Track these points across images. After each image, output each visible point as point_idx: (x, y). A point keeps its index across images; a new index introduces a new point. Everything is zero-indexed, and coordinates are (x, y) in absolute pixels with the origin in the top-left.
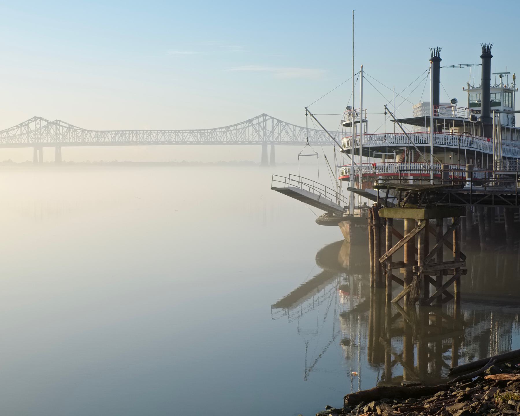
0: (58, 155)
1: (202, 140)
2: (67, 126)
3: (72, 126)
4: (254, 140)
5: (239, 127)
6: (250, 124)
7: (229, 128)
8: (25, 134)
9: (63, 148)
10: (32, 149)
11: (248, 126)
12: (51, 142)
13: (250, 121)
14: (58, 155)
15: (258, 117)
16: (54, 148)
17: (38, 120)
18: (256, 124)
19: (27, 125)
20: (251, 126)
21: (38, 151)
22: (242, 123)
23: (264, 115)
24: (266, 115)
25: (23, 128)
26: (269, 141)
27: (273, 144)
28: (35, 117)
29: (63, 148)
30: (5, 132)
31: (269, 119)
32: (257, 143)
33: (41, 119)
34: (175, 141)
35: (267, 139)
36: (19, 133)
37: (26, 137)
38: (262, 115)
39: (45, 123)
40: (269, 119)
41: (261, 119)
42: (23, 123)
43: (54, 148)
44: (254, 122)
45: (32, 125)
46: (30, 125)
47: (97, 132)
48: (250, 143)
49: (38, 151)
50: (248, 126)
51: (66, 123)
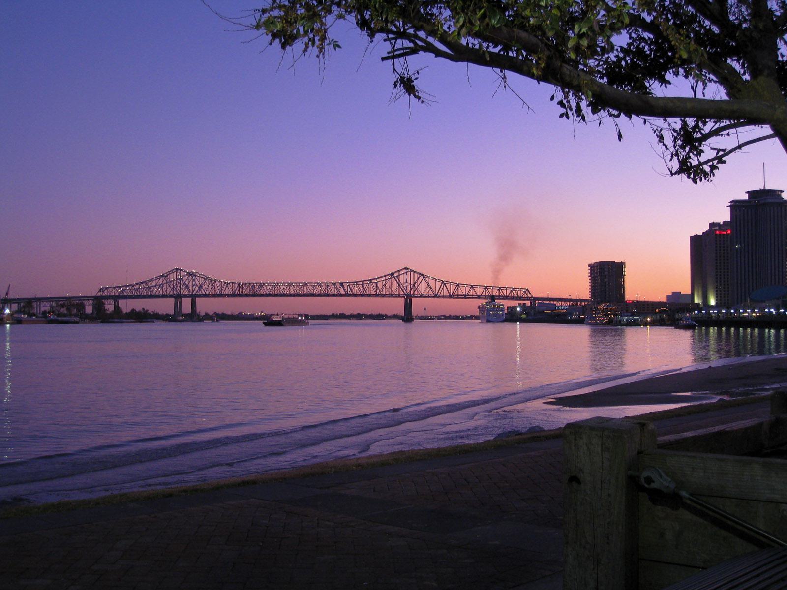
0: (194, 304)
4: (331, 293)
8: (165, 283)
10: (173, 300)
13: (392, 274)
14: (194, 304)
16: (190, 299)
17: (179, 271)
23: (406, 269)
25: (163, 278)
27: (414, 296)
32: (399, 296)
33: (181, 270)
34: (275, 294)
37: (170, 289)
41: (405, 271)
42: (162, 276)
43: (190, 299)
45: (172, 277)
48: (392, 296)
50: (391, 278)
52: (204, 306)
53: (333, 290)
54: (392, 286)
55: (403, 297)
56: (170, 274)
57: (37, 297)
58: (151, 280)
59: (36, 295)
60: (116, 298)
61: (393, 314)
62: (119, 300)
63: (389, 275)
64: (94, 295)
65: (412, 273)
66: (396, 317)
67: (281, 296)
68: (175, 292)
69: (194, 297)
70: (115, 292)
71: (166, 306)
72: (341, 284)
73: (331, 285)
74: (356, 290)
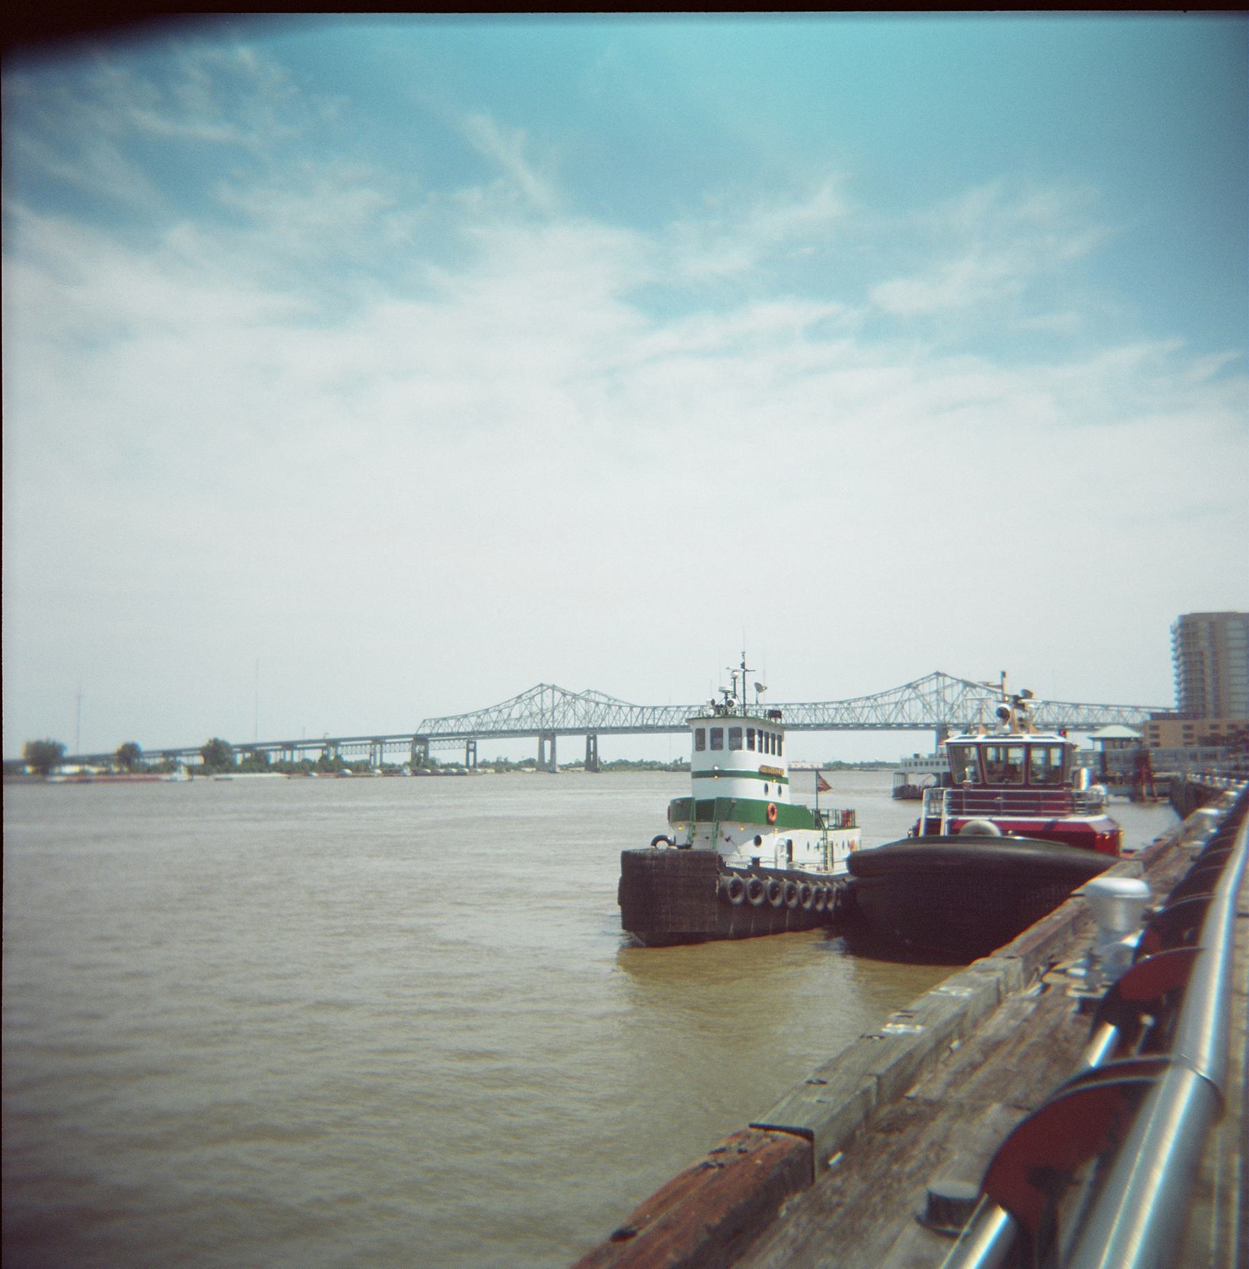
2: (604, 700)
6: (913, 695)
7: (875, 700)
9: (600, 738)
11: (909, 699)
15: (927, 679)
16: (583, 738)
18: (931, 693)
19: (532, 698)
20: (914, 699)
21: (547, 744)
22: (896, 691)
23: (938, 674)
24: (945, 675)
28: (541, 685)
29: (600, 738)
30: (495, 711)
31: (951, 686)
32: (928, 727)
33: (553, 688)
36: (515, 714)
39: (558, 695)
40: (951, 686)
42: (520, 697)
43: (583, 738)
45: (538, 698)
46: (536, 698)
48: (914, 726)
49: (547, 744)
51: (605, 696)
52: (610, 748)
54: (915, 712)
55: (933, 728)
56: (923, 683)
57: (328, 737)
58: (882, 695)
59: (327, 734)
60: (470, 738)
61: (455, 762)
62: (478, 741)
63: (909, 686)
64: (413, 732)
65: (597, 695)
66: (578, 764)
67: (814, 729)
68: (813, 719)
69: (592, 734)
70: (467, 726)
71: (527, 748)
73: (1100, 710)
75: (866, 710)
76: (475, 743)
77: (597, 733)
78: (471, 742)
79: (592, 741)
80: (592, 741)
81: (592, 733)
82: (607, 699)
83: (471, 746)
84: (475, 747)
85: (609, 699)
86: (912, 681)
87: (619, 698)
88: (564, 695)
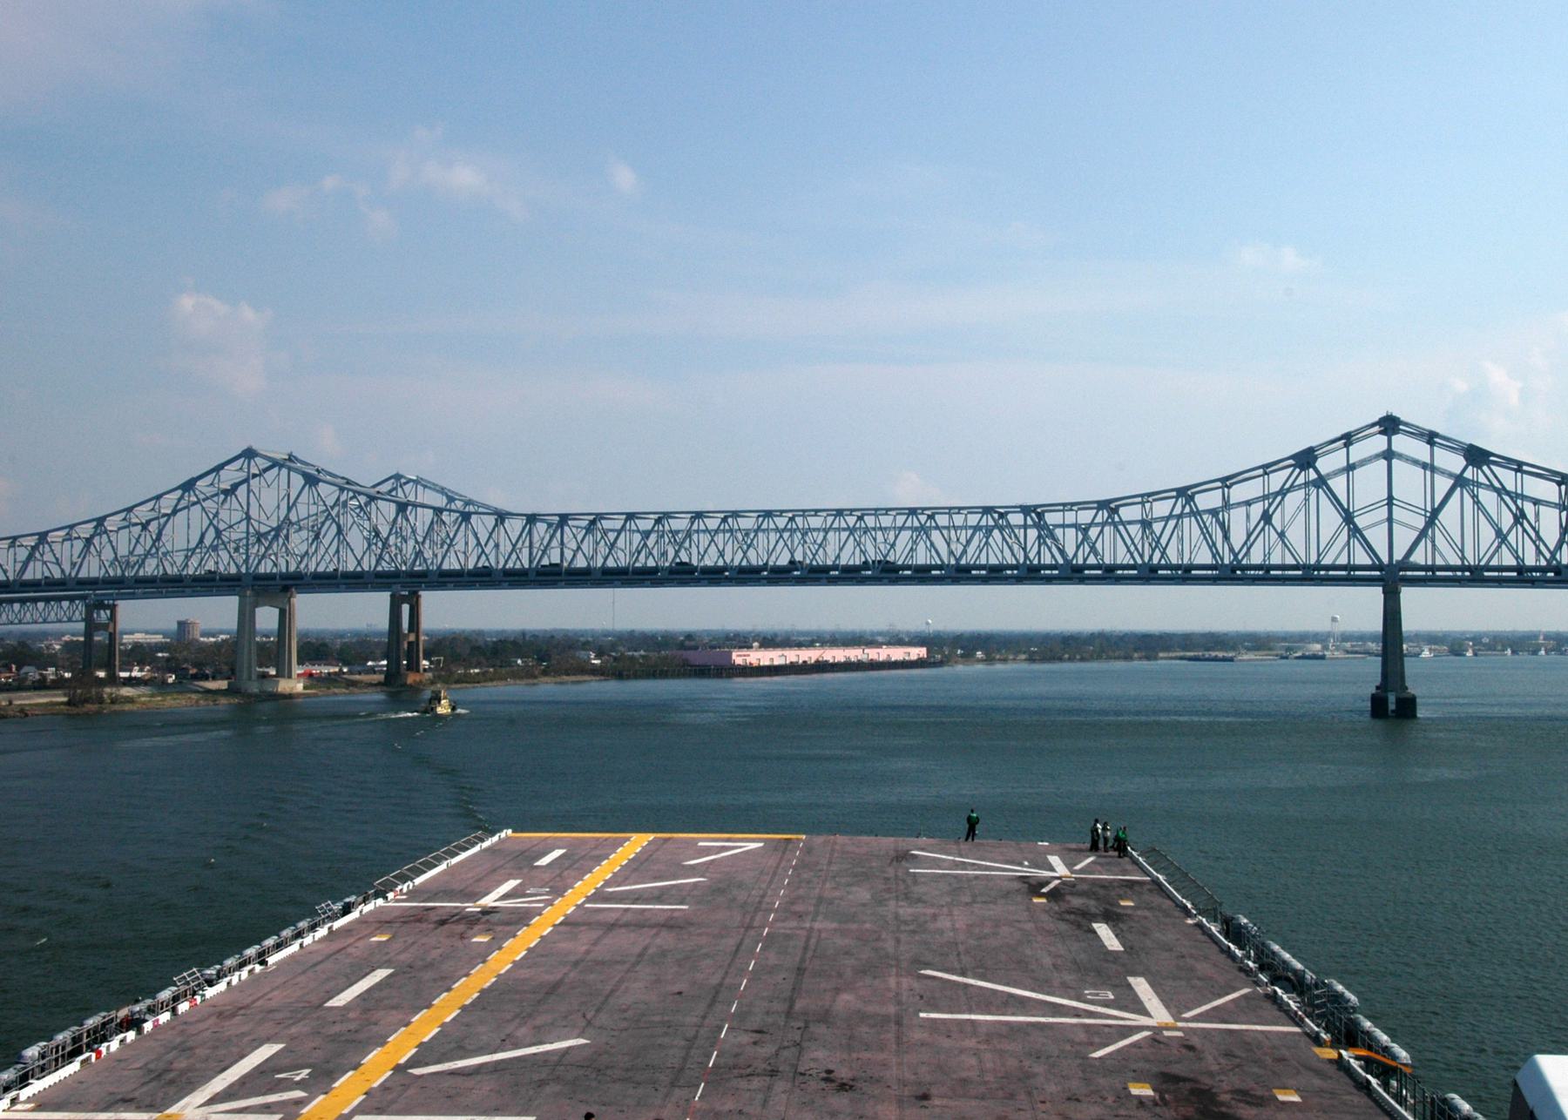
1: (1047, 560)
3: (468, 503)
5: (1238, 493)
12: (379, 568)
13: (1306, 459)
23: (1390, 425)
26: (1163, 562)
33: (288, 463)
35: (1157, 555)
38: (1380, 422)
42: (188, 486)
44: (1325, 464)
47: (532, 519)
51: (442, 491)
53: (997, 552)
72: (1034, 513)
74: (1114, 550)
75: (906, 535)
76: (113, 608)
77: (419, 586)
78: (105, 607)
79: (406, 608)
80: (406, 608)
81: (404, 586)
82: (445, 500)
83: (104, 615)
84: (113, 618)
85: (451, 500)
86: (1314, 445)
87: (475, 498)
88: (311, 480)
